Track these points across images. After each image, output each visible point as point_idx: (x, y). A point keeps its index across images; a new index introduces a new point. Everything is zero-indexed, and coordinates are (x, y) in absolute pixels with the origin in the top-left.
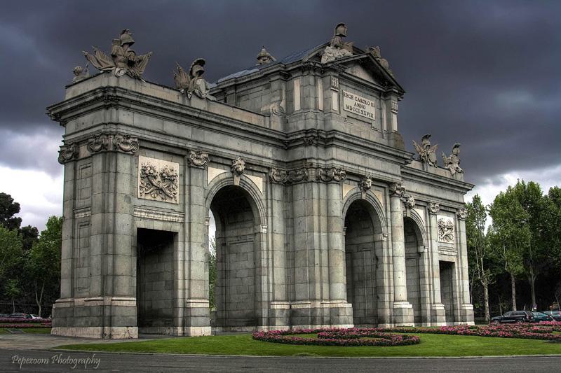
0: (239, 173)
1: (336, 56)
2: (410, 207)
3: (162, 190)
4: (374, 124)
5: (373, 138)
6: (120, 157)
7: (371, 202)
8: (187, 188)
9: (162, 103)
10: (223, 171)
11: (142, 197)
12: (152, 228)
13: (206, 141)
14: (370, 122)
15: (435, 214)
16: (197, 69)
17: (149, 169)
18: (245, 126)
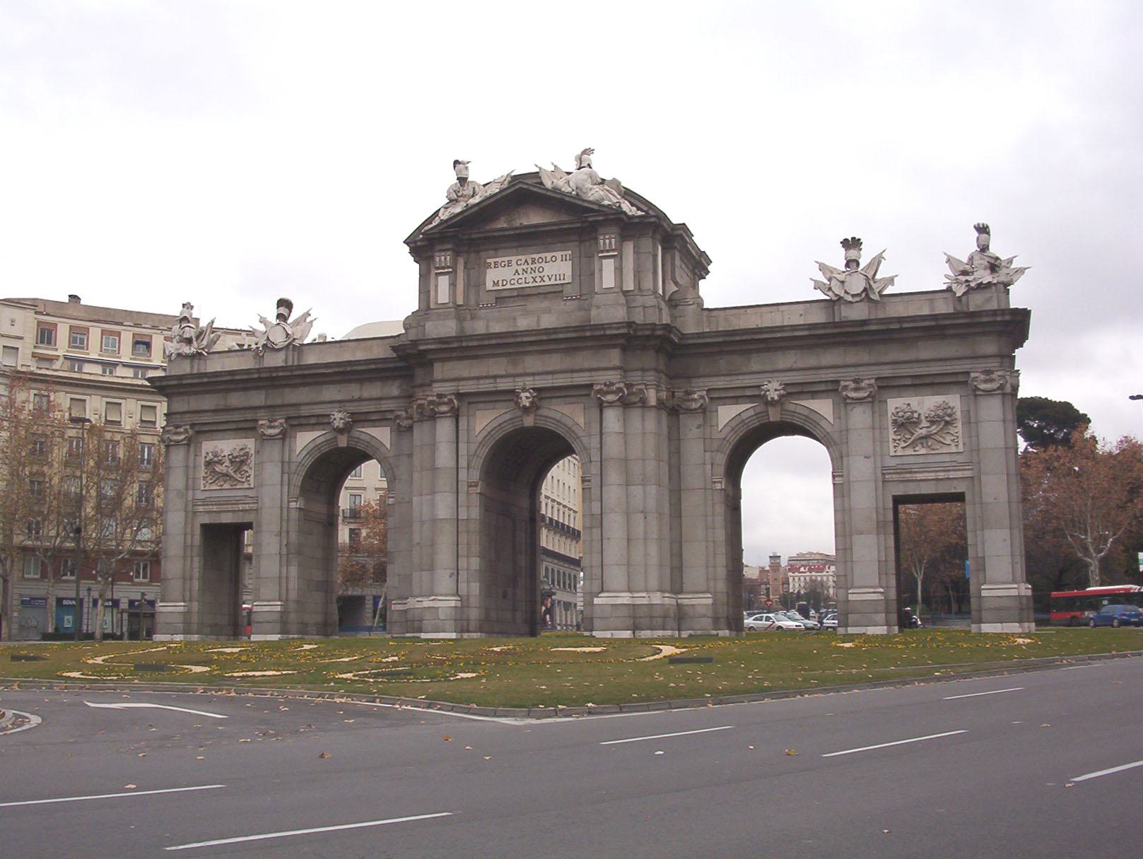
0: (339, 431)
1: (442, 218)
2: (773, 403)
3: (227, 475)
4: (568, 291)
5: (548, 322)
6: (172, 450)
7: (551, 426)
8: (260, 464)
9: (208, 377)
10: (324, 432)
11: (207, 488)
12: (218, 522)
13: (286, 403)
14: (561, 289)
15: (874, 400)
16: (283, 310)
17: (210, 454)
18: (331, 367)
